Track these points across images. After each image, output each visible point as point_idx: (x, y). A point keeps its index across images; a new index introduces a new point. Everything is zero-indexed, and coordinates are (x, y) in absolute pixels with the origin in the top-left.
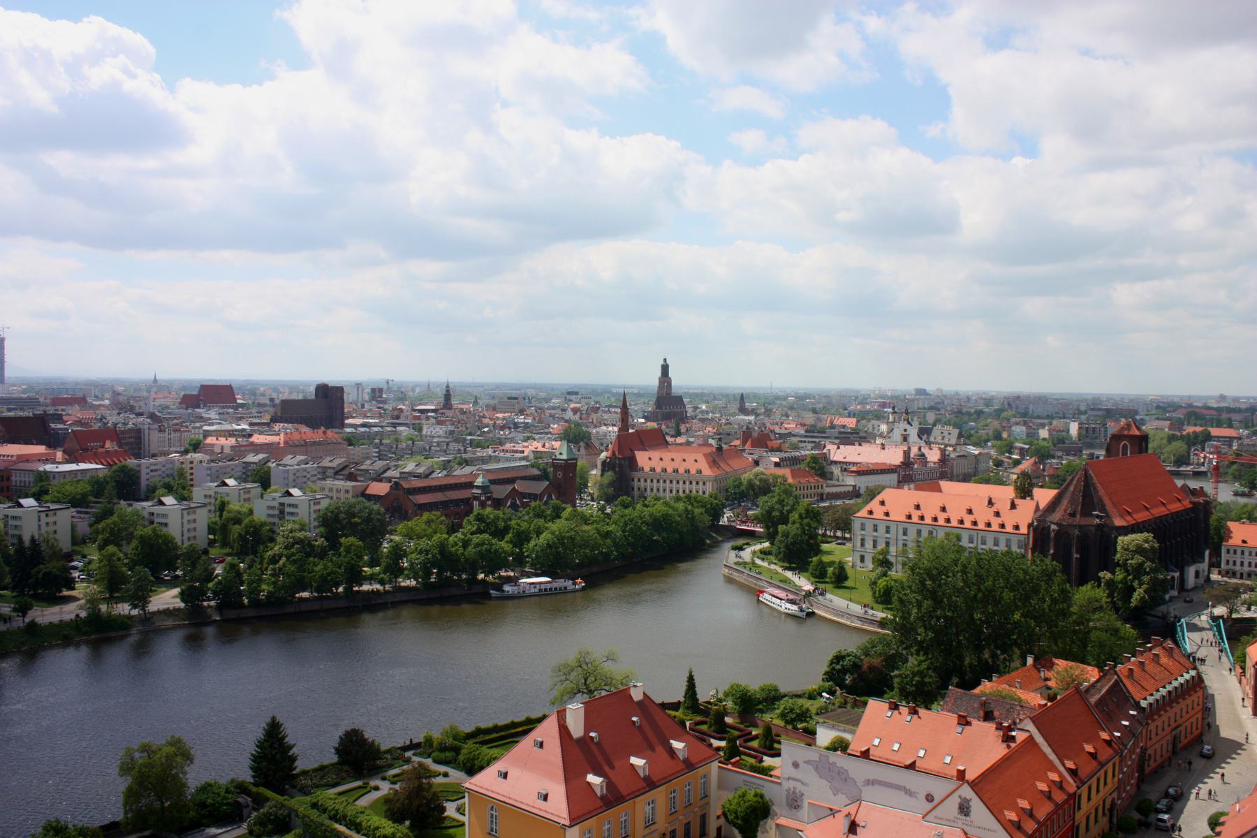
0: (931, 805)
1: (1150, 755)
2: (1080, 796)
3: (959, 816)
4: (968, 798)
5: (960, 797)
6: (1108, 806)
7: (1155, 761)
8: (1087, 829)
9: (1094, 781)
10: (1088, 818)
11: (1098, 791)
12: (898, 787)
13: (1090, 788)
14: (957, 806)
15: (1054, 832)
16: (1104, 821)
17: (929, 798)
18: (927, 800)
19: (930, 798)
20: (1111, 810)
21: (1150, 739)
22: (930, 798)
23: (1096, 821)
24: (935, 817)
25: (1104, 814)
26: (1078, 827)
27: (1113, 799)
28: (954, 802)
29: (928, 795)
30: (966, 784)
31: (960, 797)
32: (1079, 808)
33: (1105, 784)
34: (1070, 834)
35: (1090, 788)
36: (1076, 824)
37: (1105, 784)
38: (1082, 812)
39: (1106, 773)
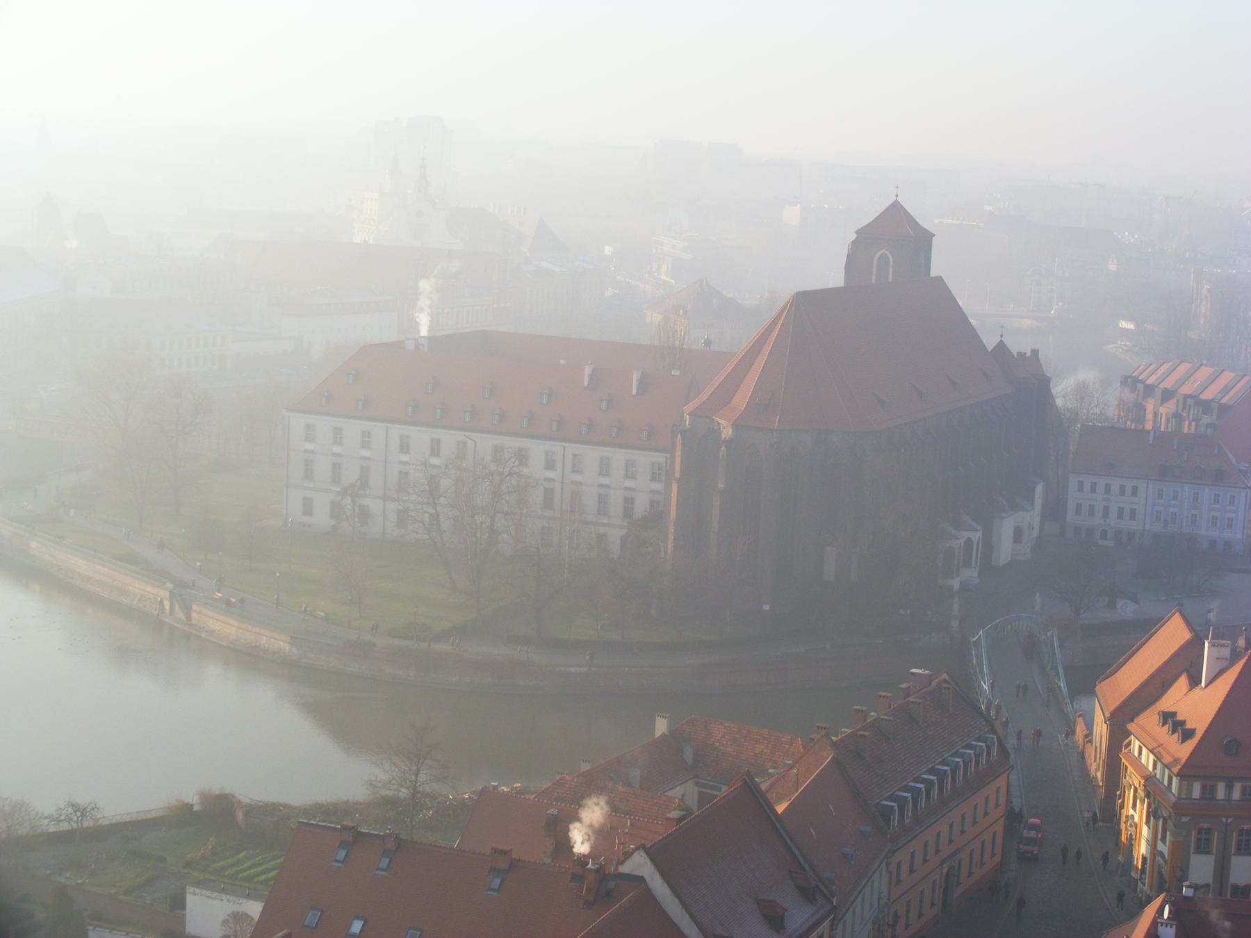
1: (896, 915)
7: (907, 926)
21: (899, 881)
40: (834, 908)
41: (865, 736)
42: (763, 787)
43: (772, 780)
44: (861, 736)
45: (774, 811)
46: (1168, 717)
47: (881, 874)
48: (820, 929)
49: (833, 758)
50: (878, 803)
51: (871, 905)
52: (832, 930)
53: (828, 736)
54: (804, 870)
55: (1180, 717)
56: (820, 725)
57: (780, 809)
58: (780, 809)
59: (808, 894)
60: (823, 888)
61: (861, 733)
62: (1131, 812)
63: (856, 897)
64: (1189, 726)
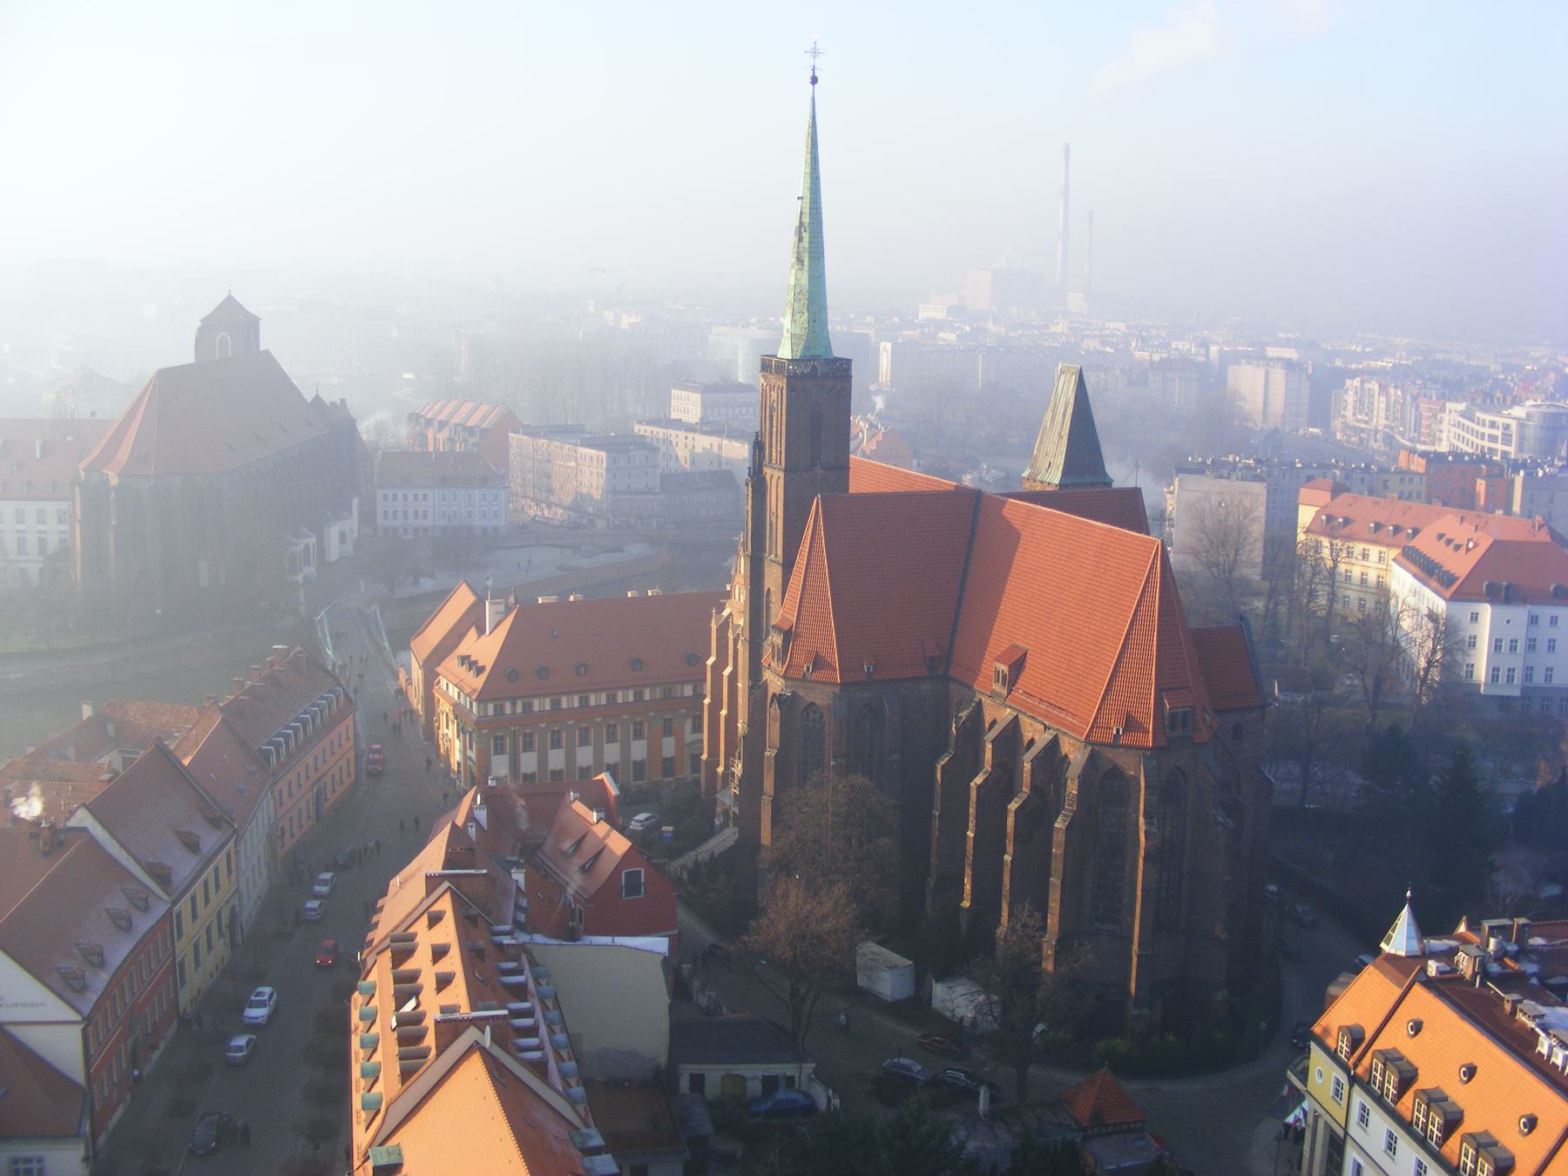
1: (283, 829)
2: (179, 916)
6: (225, 921)
7: (292, 836)
8: (197, 963)
9: (198, 887)
11: (207, 900)
13: (193, 899)
15: (143, 982)
16: (221, 947)
20: (231, 926)
21: (281, 804)
23: (210, 947)
25: (221, 934)
26: (182, 964)
27: (233, 908)
32: (180, 935)
33: (218, 887)
34: (171, 978)
35: (193, 899)
36: (178, 960)
37: (218, 887)
38: (184, 939)
39: (216, 870)
40: (236, 830)
43: (178, 741)
44: (242, 700)
46: (464, 659)
52: (236, 846)
53: (216, 702)
55: (473, 659)
57: (186, 762)
58: (186, 762)
59: (215, 823)
60: (227, 818)
61: (240, 698)
62: (446, 731)
63: (252, 819)
64: (480, 664)
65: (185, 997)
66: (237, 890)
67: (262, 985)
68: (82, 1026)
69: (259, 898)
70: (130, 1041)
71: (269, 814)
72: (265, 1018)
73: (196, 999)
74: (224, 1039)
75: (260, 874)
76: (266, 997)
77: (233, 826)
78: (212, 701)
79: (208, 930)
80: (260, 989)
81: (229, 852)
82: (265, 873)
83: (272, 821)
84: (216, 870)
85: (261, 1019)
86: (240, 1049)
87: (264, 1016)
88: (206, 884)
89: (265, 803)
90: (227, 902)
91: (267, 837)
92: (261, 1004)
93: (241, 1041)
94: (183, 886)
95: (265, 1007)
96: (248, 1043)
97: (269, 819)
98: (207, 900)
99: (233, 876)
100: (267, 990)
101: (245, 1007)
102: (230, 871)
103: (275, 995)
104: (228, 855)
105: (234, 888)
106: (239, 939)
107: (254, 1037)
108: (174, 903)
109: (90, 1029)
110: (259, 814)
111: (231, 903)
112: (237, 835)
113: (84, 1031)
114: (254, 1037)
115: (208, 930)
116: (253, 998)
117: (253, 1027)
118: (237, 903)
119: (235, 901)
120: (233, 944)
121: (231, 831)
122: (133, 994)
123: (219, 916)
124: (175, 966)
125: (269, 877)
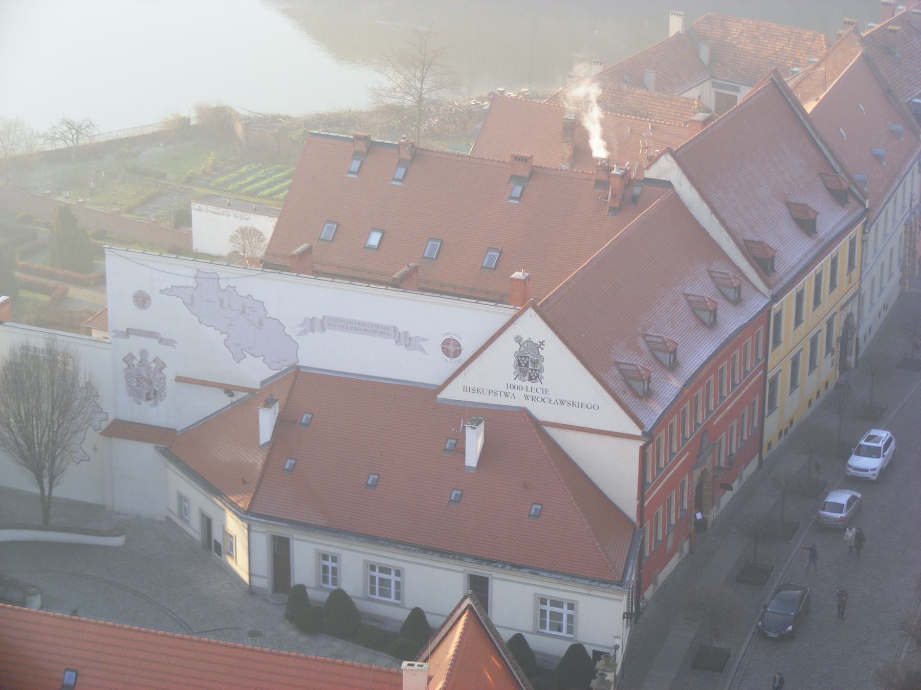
0: (455, 364)
2: (778, 317)
3: (518, 382)
4: (536, 341)
5: (518, 339)
6: (837, 332)
8: (794, 384)
9: (808, 282)
10: (795, 363)
11: (817, 301)
12: (381, 331)
13: (800, 297)
14: (513, 360)
15: (722, 398)
16: (827, 367)
17: (451, 348)
18: (446, 352)
19: (451, 348)
20: (844, 341)
22: (451, 348)
23: (813, 365)
24: (465, 389)
25: (829, 349)
27: (850, 316)
28: (507, 349)
29: (446, 342)
30: (530, 312)
31: (518, 339)
32: (777, 342)
33: (833, 285)
35: (800, 297)
36: (770, 376)
37: (833, 285)
38: (781, 349)
39: (834, 261)
40: (867, 210)
41: (895, 31)
42: (791, 84)
43: (797, 79)
44: (891, 30)
45: (803, 111)
47: (913, 175)
48: (852, 233)
49: (863, 54)
50: (910, 101)
51: (903, 207)
52: (864, 233)
53: (856, 31)
54: (835, 171)
56: (847, 19)
57: (810, 107)
58: (810, 107)
59: (840, 196)
60: (856, 191)
61: (890, 27)
63: (889, 200)
65: (772, 426)
66: (858, 293)
67: (878, 428)
68: (641, 443)
69: (885, 307)
70: (697, 474)
71: (912, 194)
72: (877, 472)
73: (786, 431)
74: (818, 491)
75: (891, 275)
76: (881, 444)
77: (864, 205)
78: (852, 28)
79: (814, 342)
80: (873, 432)
81: (855, 238)
82: (897, 275)
83: (914, 204)
84: (834, 261)
85: (870, 473)
86: (838, 508)
87: (874, 469)
88: (818, 278)
89: (909, 177)
90: (842, 308)
91: (906, 225)
92: (873, 453)
93: (841, 497)
94: (787, 279)
95: (879, 457)
96: (850, 502)
97: (911, 200)
98: (817, 301)
99: (855, 273)
100: (884, 435)
101: (850, 454)
102: (851, 266)
103: (893, 443)
104: (852, 243)
105: (852, 292)
106: (851, 360)
107: (859, 495)
108: (775, 298)
109: (650, 450)
110: (900, 191)
111: (849, 309)
112: (867, 218)
113: (643, 450)
114: (859, 495)
115: (814, 342)
116: (863, 442)
117: (856, 481)
118: (855, 310)
119: (853, 308)
120: (843, 366)
121: (861, 210)
122: (709, 412)
123: (830, 324)
124: (765, 384)
125: (902, 282)
